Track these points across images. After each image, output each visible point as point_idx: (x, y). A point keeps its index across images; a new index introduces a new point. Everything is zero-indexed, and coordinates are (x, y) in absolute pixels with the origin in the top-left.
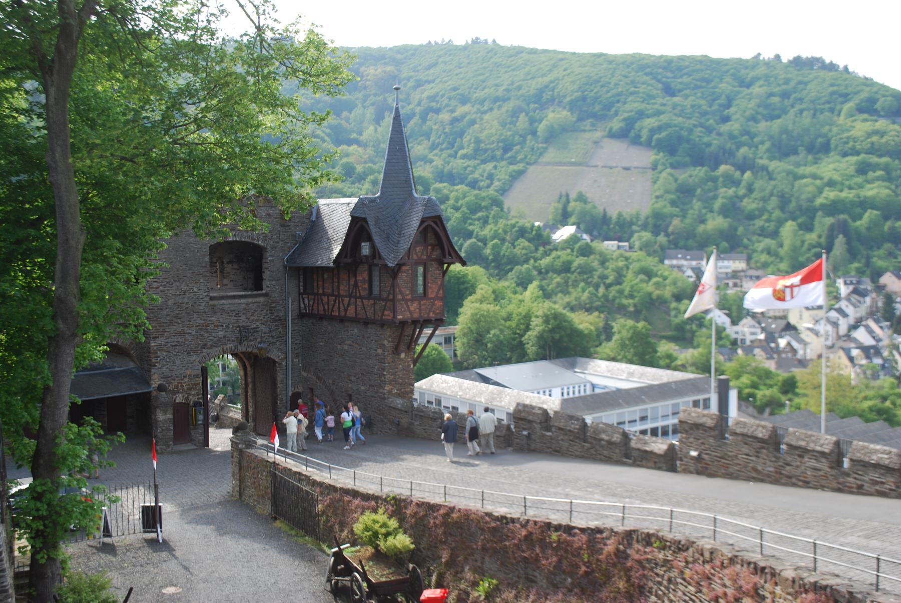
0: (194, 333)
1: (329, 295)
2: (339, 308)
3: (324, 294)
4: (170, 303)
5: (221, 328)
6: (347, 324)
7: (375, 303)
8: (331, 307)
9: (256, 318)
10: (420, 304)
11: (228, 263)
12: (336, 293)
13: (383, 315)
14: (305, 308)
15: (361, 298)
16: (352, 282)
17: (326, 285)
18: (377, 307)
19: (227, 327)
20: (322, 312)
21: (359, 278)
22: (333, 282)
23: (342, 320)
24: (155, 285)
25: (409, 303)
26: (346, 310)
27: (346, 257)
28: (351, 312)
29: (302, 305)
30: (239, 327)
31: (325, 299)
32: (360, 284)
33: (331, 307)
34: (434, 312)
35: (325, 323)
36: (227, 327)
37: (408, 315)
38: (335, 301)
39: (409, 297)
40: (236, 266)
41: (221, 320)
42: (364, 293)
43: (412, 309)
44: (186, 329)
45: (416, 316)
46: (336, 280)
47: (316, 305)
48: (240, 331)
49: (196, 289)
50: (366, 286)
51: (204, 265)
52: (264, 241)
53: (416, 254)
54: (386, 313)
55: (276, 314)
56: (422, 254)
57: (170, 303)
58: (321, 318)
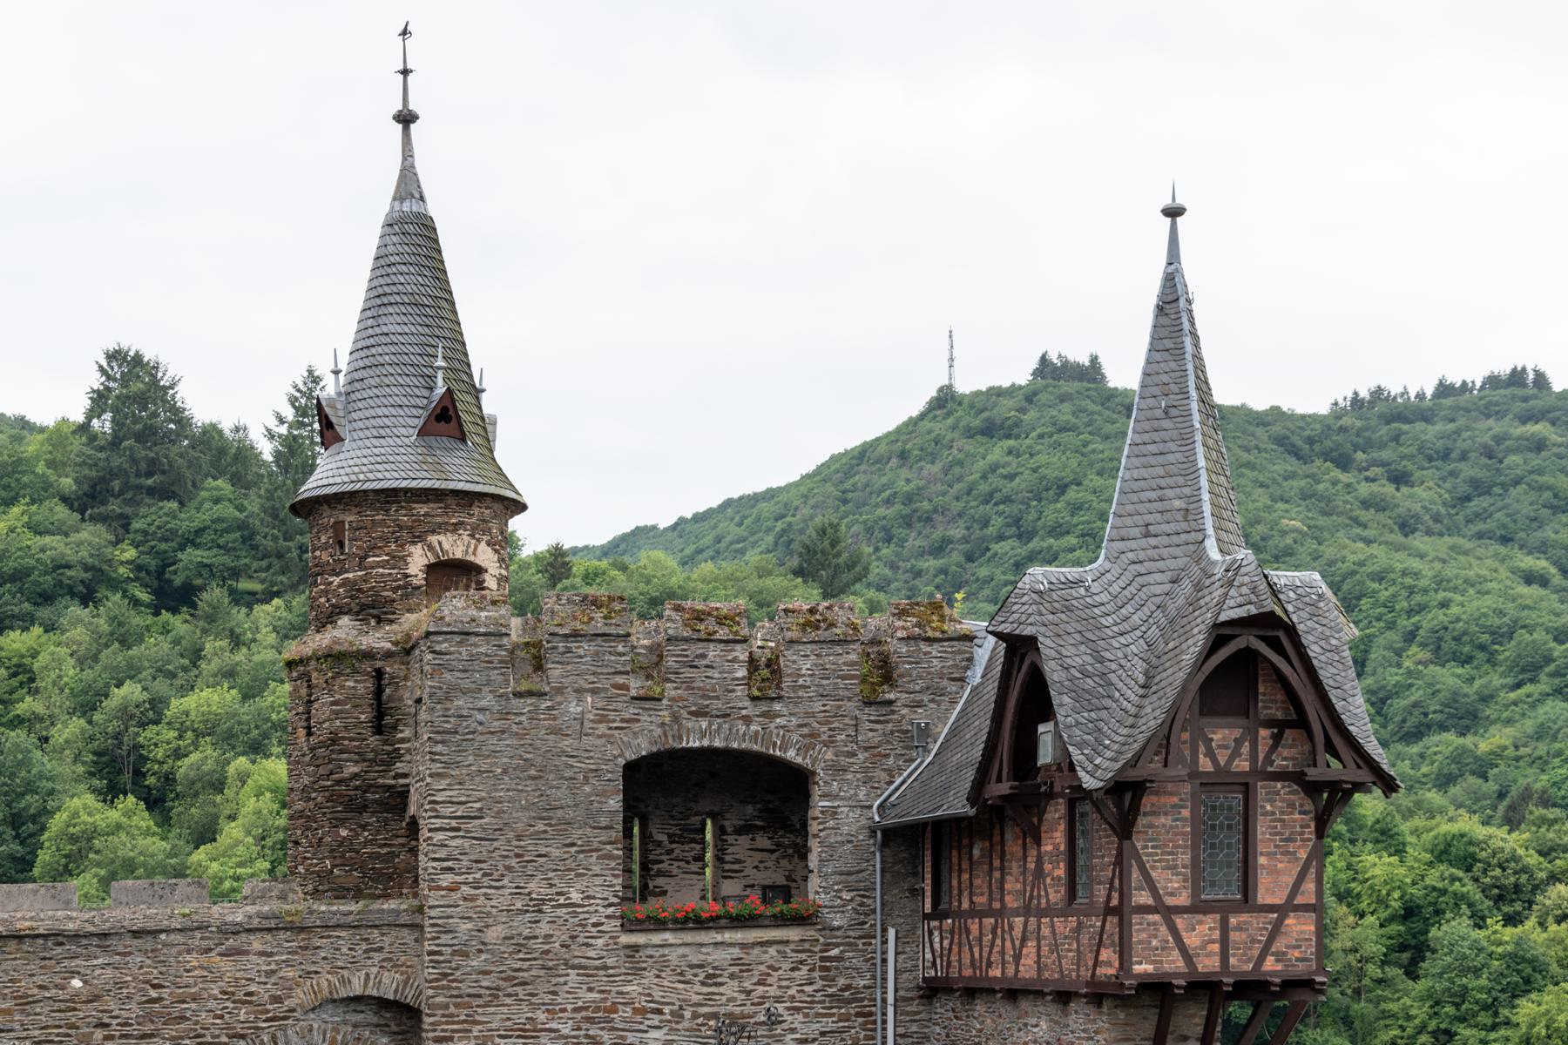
0: (566, 1029)
1: (981, 915)
2: (1003, 953)
3: (975, 913)
4: (493, 934)
5: (655, 1020)
6: (1024, 1004)
7: (1079, 928)
8: (985, 954)
9: (773, 991)
10: (1225, 928)
11: (739, 831)
12: (997, 905)
13: (1096, 963)
14: (934, 963)
15: (1046, 912)
16: (1031, 866)
17: (977, 882)
18: (1085, 939)
19: (678, 1015)
20: (967, 972)
21: (1047, 848)
22: (991, 869)
23: (1014, 994)
24: (446, 880)
25: (1180, 922)
26: (1017, 958)
27: (999, 780)
28: (1028, 970)
29: (929, 956)
30: (715, 1016)
31: (974, 926)
32: (1047, 867)
33: (985, 954)
34: (1280, 957)
35: (980, 1007)
36: (678, 1015)
37: (1174, 963)
38: (994, 931)
39: (1183, 899)
40: (763, 841)
41: (657, 994)
42: (1056, 895)
43: (1192, 940)
44: (542, 1017)
45: (1208, 964)
46: (997, 863)
47: (955, 948)
48: (719, 1030)
49: (576, 897)
50: (1061, 872)
51: (604, 821)
52: (804, 750)
53: (1210, 754)
54: (1105, 954)
55: (841, 982)
56: (1236, 754)
57: (493, 934)
58: (971, 992)
